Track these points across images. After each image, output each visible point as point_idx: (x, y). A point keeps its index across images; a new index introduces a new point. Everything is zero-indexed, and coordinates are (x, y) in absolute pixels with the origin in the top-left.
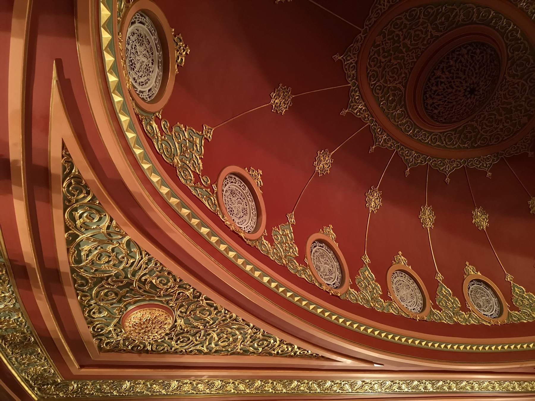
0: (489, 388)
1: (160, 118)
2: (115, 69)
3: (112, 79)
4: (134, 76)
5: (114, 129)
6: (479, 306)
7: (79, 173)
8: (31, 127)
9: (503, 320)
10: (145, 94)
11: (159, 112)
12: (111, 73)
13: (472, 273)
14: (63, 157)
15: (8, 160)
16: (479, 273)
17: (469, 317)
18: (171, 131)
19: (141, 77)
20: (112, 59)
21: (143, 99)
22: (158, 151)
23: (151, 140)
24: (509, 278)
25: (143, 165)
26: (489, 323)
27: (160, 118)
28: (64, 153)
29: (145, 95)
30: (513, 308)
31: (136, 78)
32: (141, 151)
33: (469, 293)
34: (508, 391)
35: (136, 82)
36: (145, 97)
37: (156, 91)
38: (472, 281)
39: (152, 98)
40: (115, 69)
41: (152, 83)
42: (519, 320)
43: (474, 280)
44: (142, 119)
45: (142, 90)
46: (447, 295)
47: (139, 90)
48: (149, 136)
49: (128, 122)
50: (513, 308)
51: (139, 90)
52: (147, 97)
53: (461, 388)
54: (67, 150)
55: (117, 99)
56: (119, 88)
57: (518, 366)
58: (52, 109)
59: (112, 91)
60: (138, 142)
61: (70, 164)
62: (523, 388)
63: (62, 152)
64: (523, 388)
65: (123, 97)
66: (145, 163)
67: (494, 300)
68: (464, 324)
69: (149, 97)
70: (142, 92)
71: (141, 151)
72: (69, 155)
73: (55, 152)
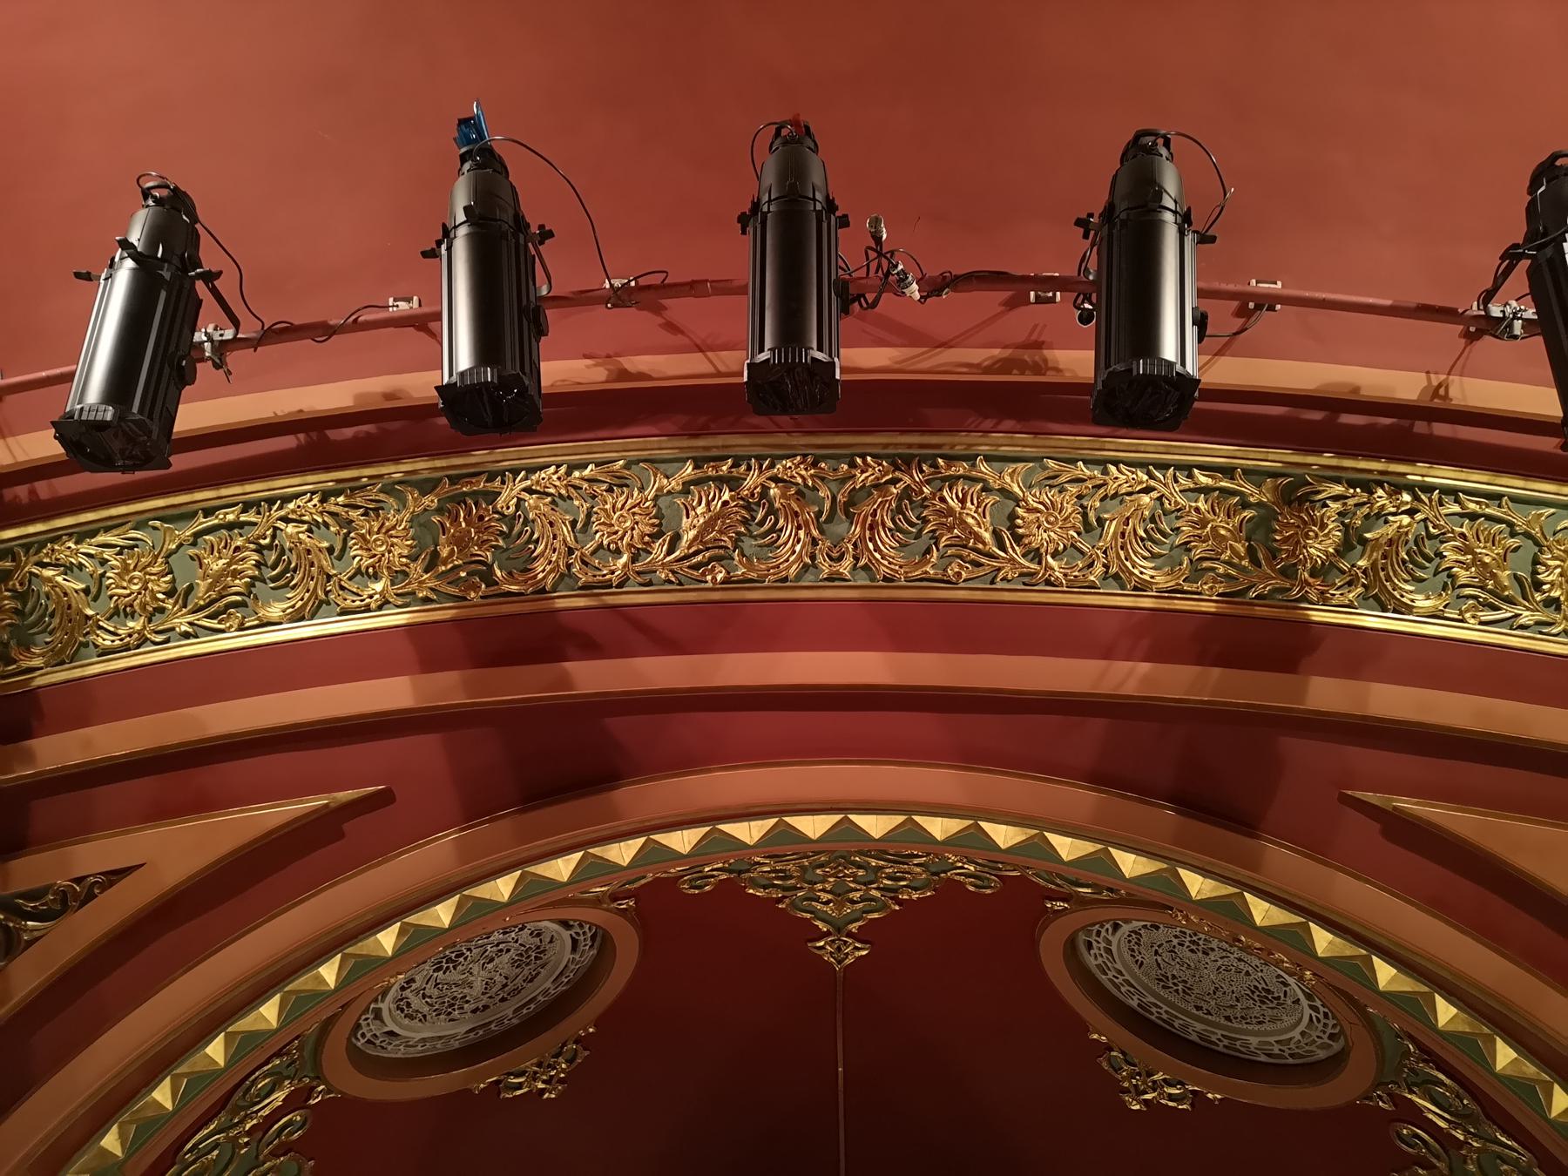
1: (312, 1102)
2: (416, 939)
3: (387, 939)
4: (417, 978)
5: (222, 1002)
7: (30, 943)
8: (162, 772)
10: (375, 1028)
11: (329, 1092)
12: (401, 933)
14: (79, 880)
15: (30, 735)
18: (274, 1154)
19: (424, 996)
20: (446, 920)
21: (358, 1026)
22: (189, 1145)
23: (223, 1108)
25: (115, 1128)
27: (312, 1102)
28: (92, 879)
29: (370, 1028)
31: (414, 986)
32: (169, 1105)
35: (403, 989)
36: (364, 1030)
37: (396, 1051)
39: (371, 1051)
40: (416, 939)
41: (416, 1033)
44: (288, 1054)
45: (385, 1014)
47: (380, 1005)
48: (236, 1097)
49: (263, 1026)
51: (380, 1005)
52: (368, 1036)
54: (104, 887)
55: (329, 973)
56: (363, 970)
58: (236, 815)
59: (349, 950)
60: (201, 1080)
61: (59, 907)
63: (94, 875)
65: (337, 989)
66: (122, 1136)
69: (369, 1042)
70: (378, 1015)
71: (169, 1105)
72: (90, 896)
73: (91, 856)
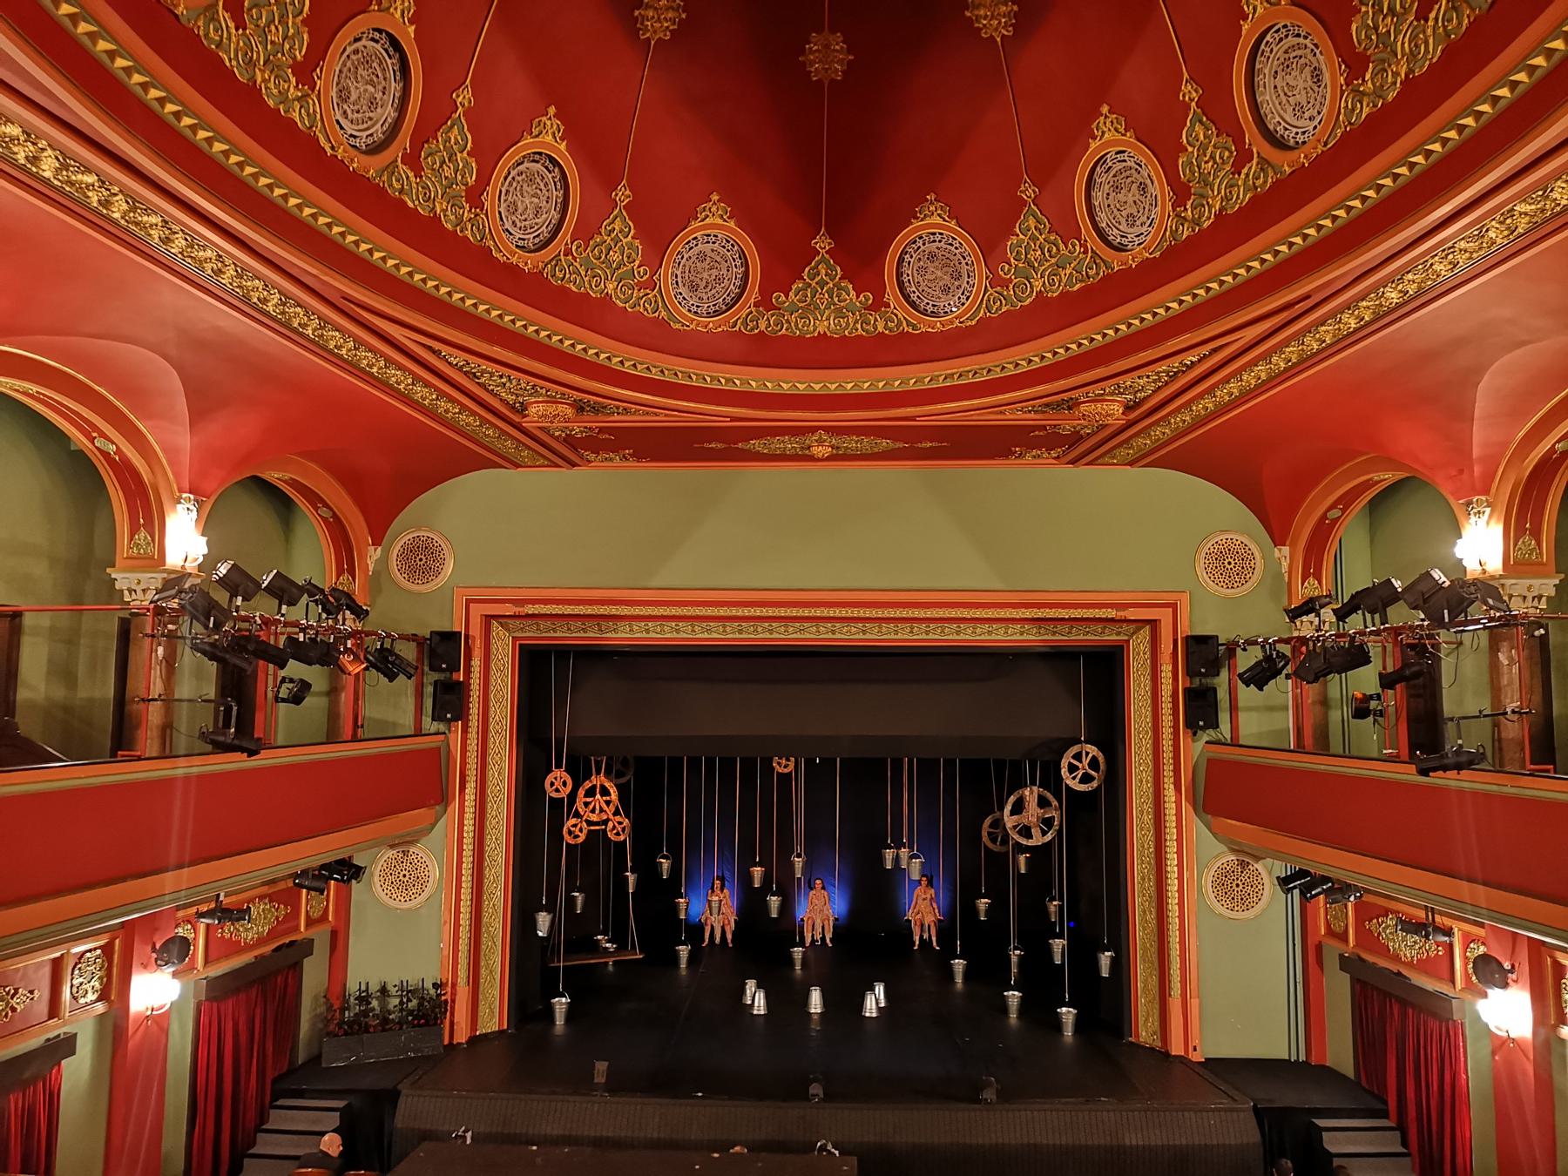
0: (208, 266)
6: (344, 96)
9: (370, 167)
13: (398, 15)
16: (412, 29)
17: (298, 99)
24: (464, 97)
26: (333, 148)
30: (413, 160)
33: (349, 49)
34: (246, 299)
38: (380, 31)
42: (401, 191)
43: (389, 35)
46: (290, 8)
50: (413, 160)
53: (137, 224)
57: (314, 271)
62: (283, 313)
64: (283, 313)
67: (388, 112)
68: (271, 103)
